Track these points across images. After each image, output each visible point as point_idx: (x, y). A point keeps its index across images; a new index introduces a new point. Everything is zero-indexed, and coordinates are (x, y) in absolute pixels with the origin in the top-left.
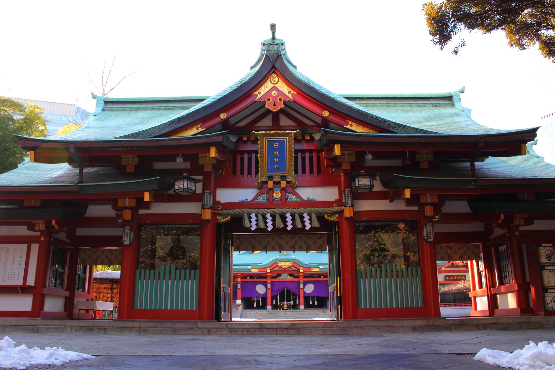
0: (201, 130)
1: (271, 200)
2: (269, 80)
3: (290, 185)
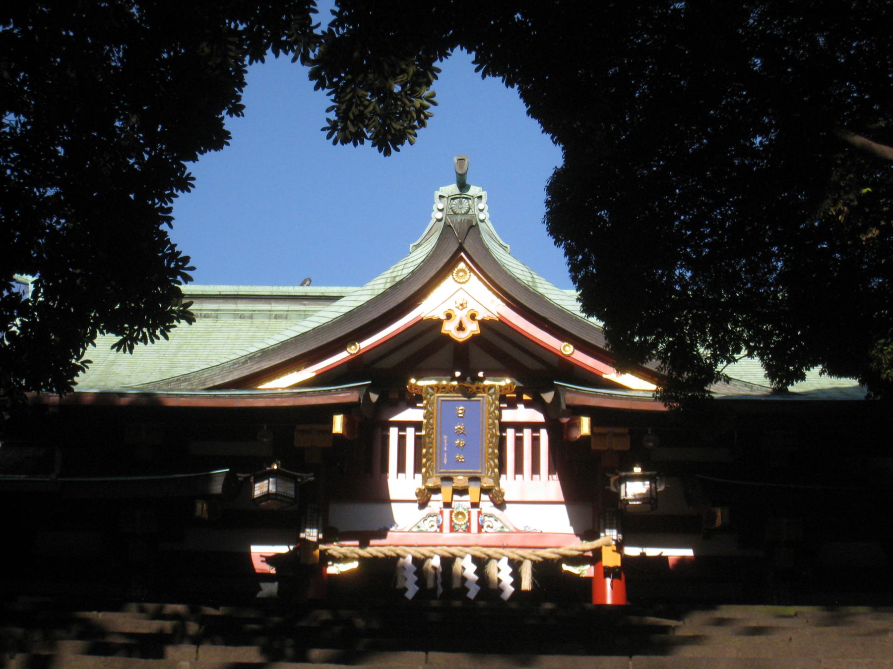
3: (490, 497)
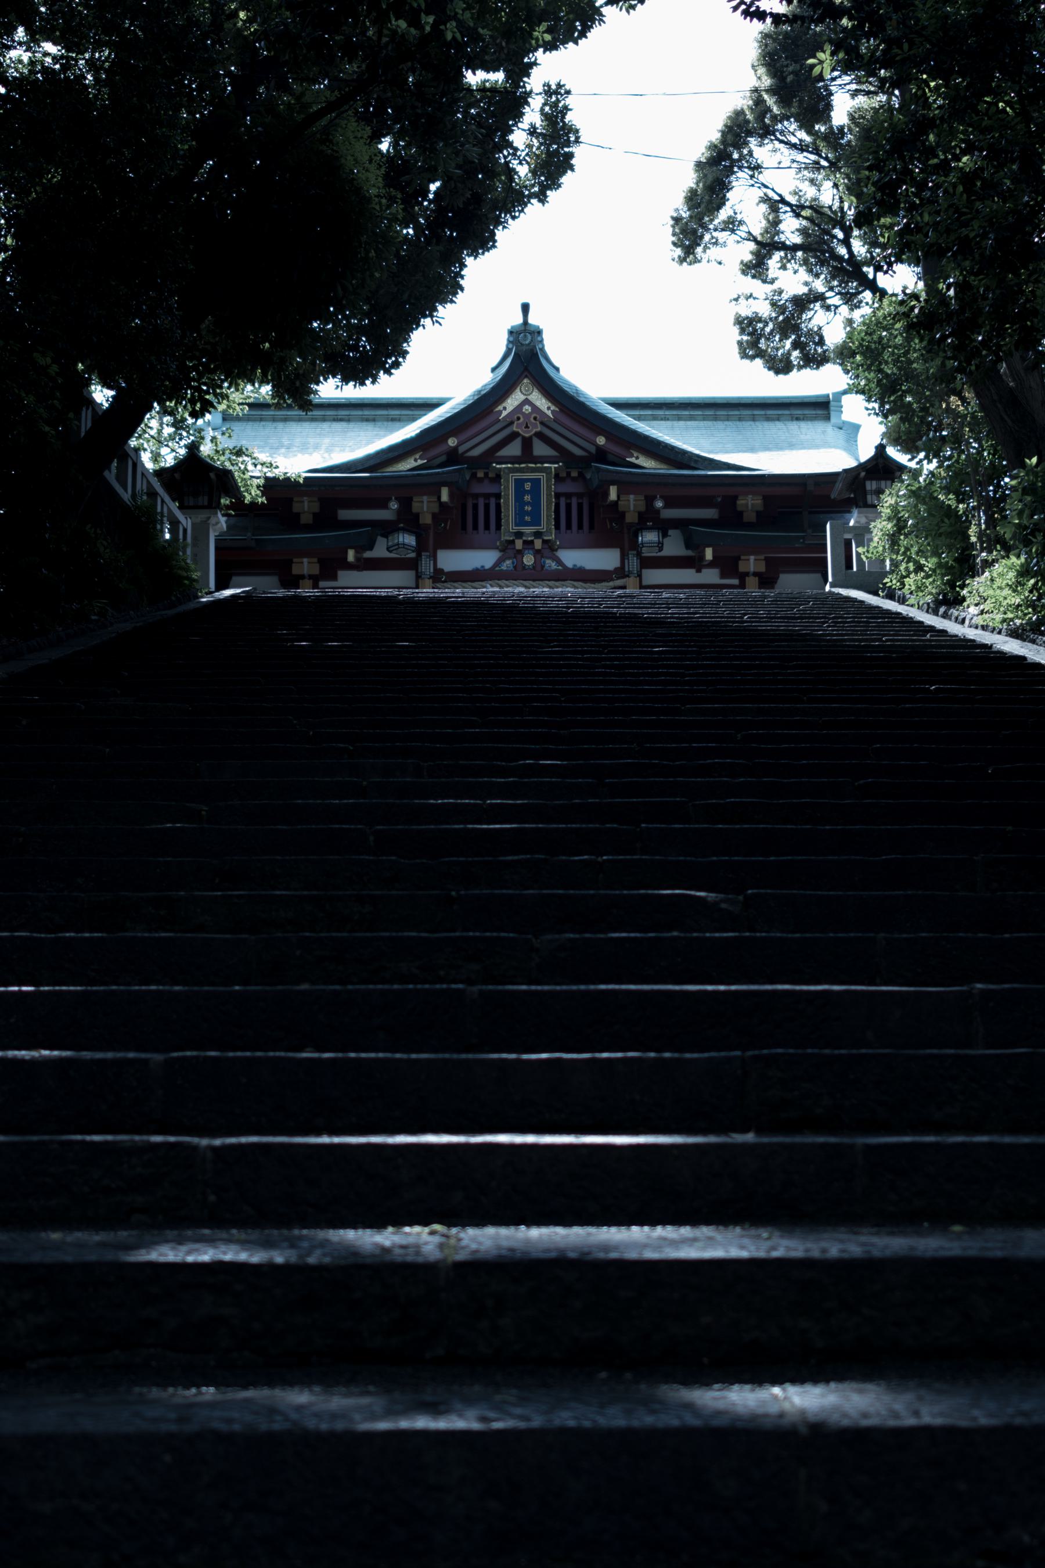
0: (420, 462)
2: (519, 388)
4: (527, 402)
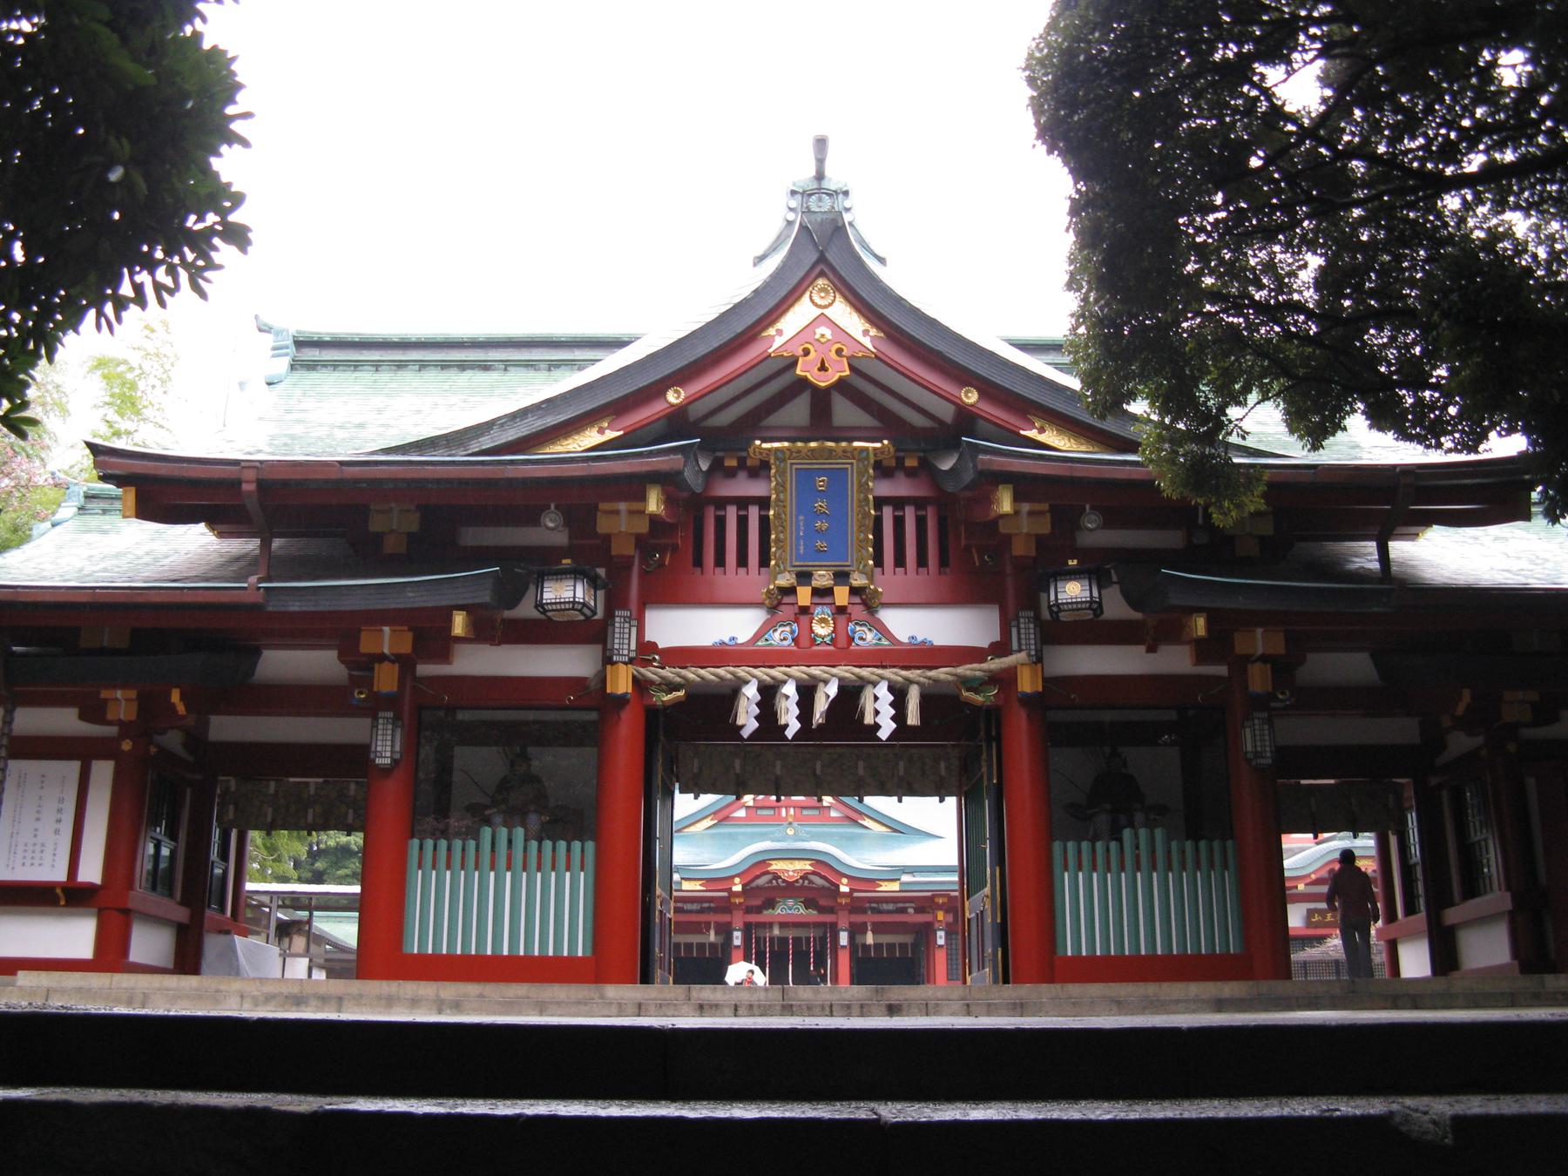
0: (610, 435)
1: (805, 642)
2: (807, 295)
3: (862, 599)
4: (822, 319)
